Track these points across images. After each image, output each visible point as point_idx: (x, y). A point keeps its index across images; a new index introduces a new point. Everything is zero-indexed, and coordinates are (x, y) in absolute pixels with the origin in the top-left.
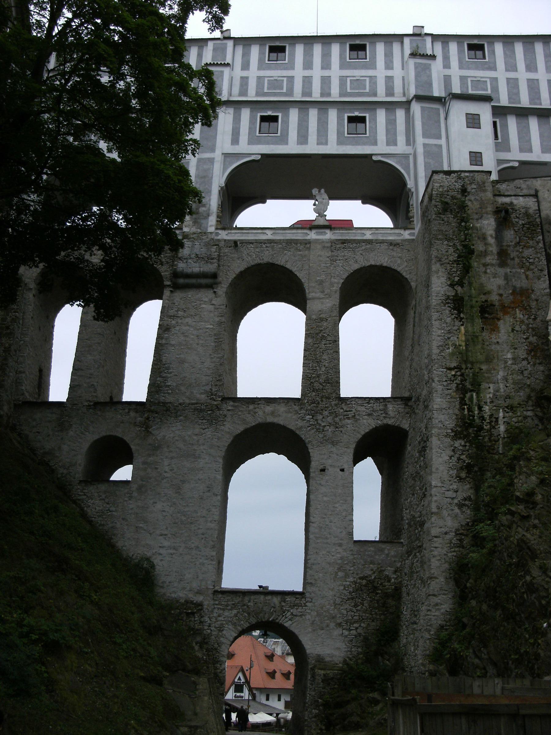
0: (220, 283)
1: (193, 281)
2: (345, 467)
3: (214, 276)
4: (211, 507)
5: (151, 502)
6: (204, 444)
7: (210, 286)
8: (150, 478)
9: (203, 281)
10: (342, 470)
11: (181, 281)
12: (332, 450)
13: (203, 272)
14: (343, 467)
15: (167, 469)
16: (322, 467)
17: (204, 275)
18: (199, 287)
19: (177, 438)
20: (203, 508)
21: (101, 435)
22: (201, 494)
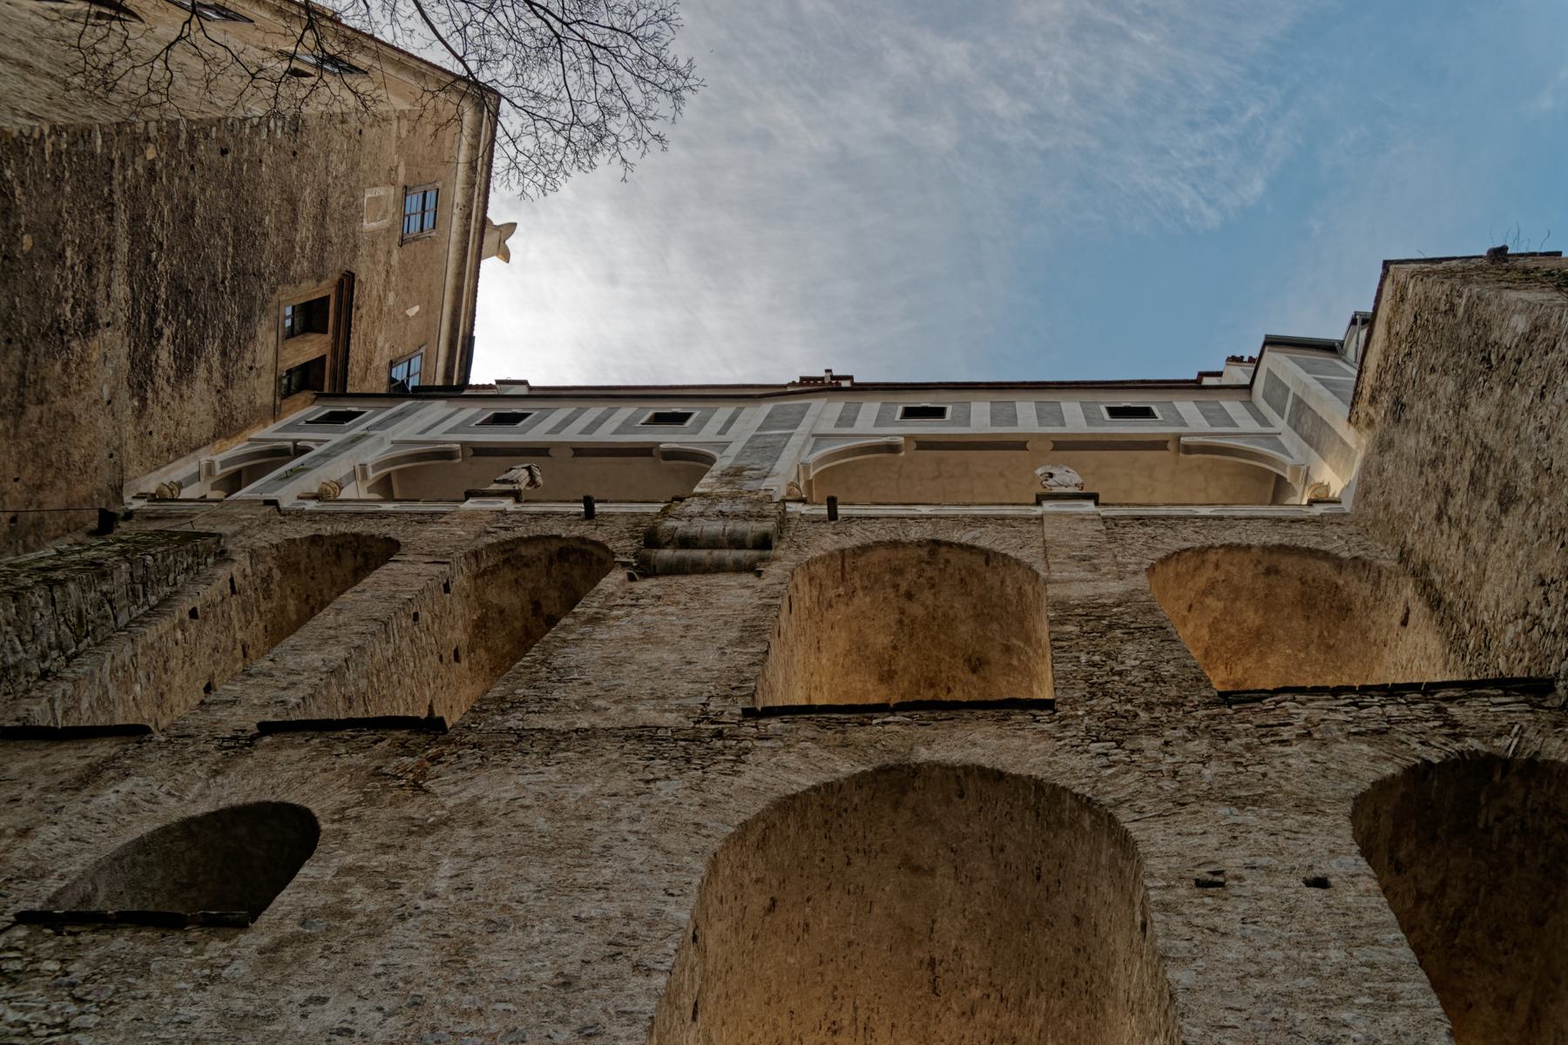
0: (776, 559)
1: (702, 554)
2: (1330, 868)
3: (764, 542)
4: (604, 1018)
5: (300, 996)
6: (633, 820)
7: (751, 568)
8: (350, 915)
9: (729, 555)
10: (1321, 883)
11: (667, 554)
12: (1240, 820)
13: (732, 533)
14: (1317, 873)
15: (441, 885)
16: (1203, 873)
17: (736, 542)
18: (719, 568)
19: (527, 802)
20: (563, 1021)
21: (222, 804)
22: (567, 969)
